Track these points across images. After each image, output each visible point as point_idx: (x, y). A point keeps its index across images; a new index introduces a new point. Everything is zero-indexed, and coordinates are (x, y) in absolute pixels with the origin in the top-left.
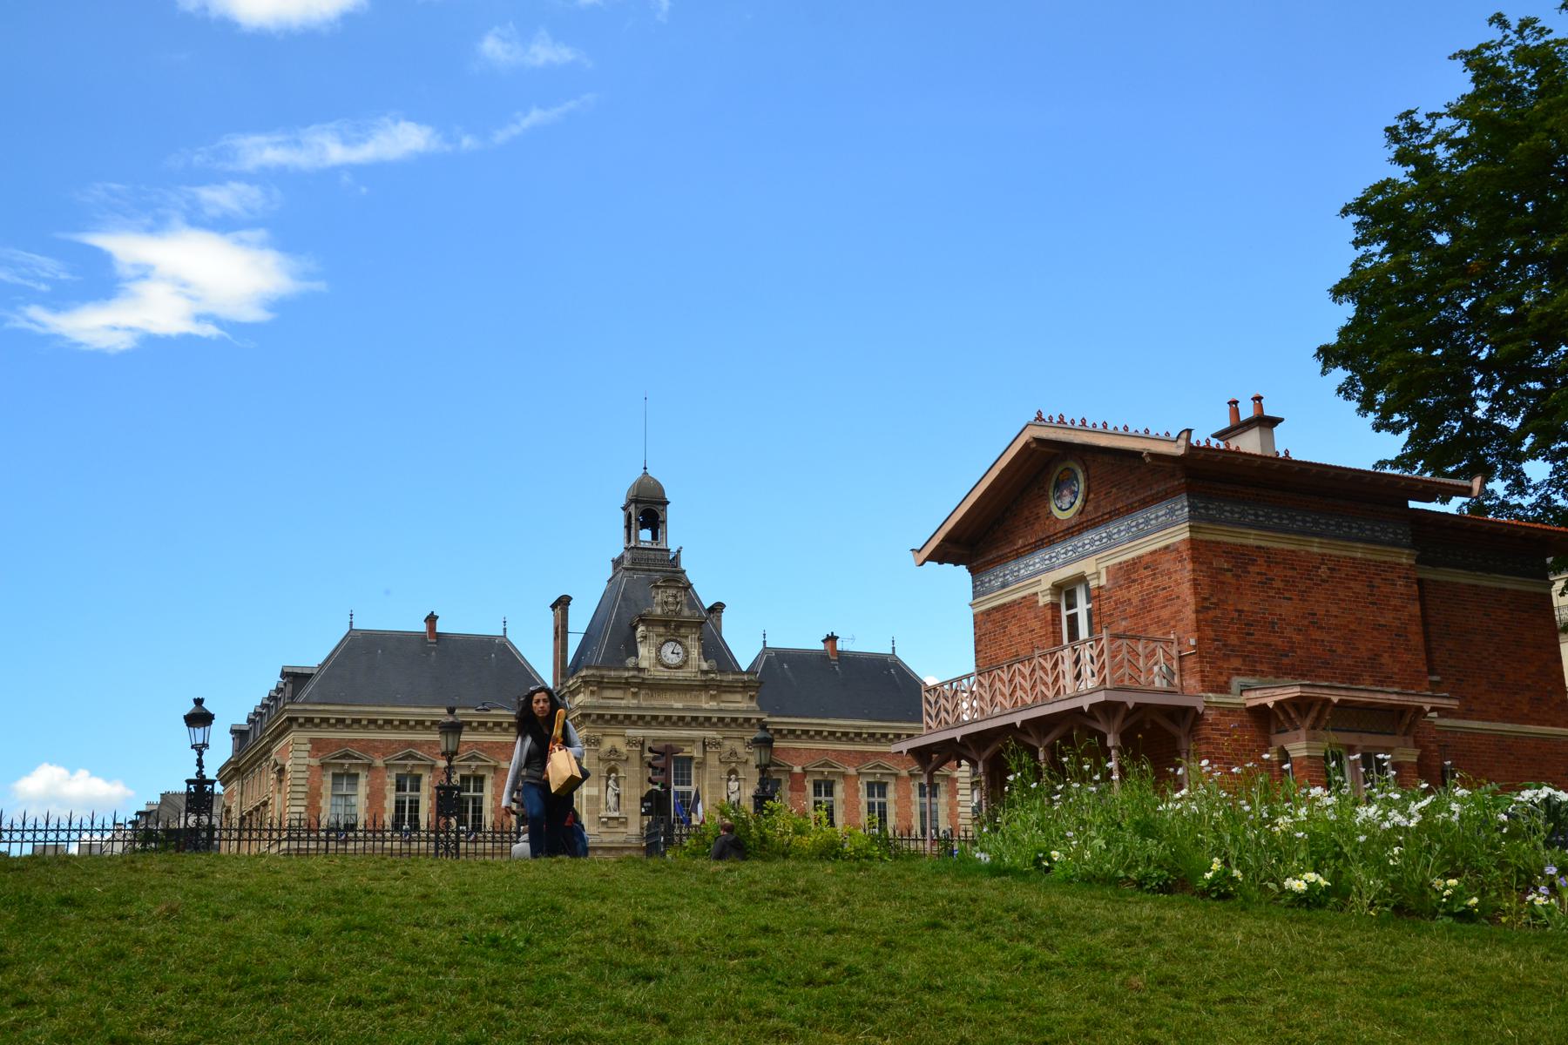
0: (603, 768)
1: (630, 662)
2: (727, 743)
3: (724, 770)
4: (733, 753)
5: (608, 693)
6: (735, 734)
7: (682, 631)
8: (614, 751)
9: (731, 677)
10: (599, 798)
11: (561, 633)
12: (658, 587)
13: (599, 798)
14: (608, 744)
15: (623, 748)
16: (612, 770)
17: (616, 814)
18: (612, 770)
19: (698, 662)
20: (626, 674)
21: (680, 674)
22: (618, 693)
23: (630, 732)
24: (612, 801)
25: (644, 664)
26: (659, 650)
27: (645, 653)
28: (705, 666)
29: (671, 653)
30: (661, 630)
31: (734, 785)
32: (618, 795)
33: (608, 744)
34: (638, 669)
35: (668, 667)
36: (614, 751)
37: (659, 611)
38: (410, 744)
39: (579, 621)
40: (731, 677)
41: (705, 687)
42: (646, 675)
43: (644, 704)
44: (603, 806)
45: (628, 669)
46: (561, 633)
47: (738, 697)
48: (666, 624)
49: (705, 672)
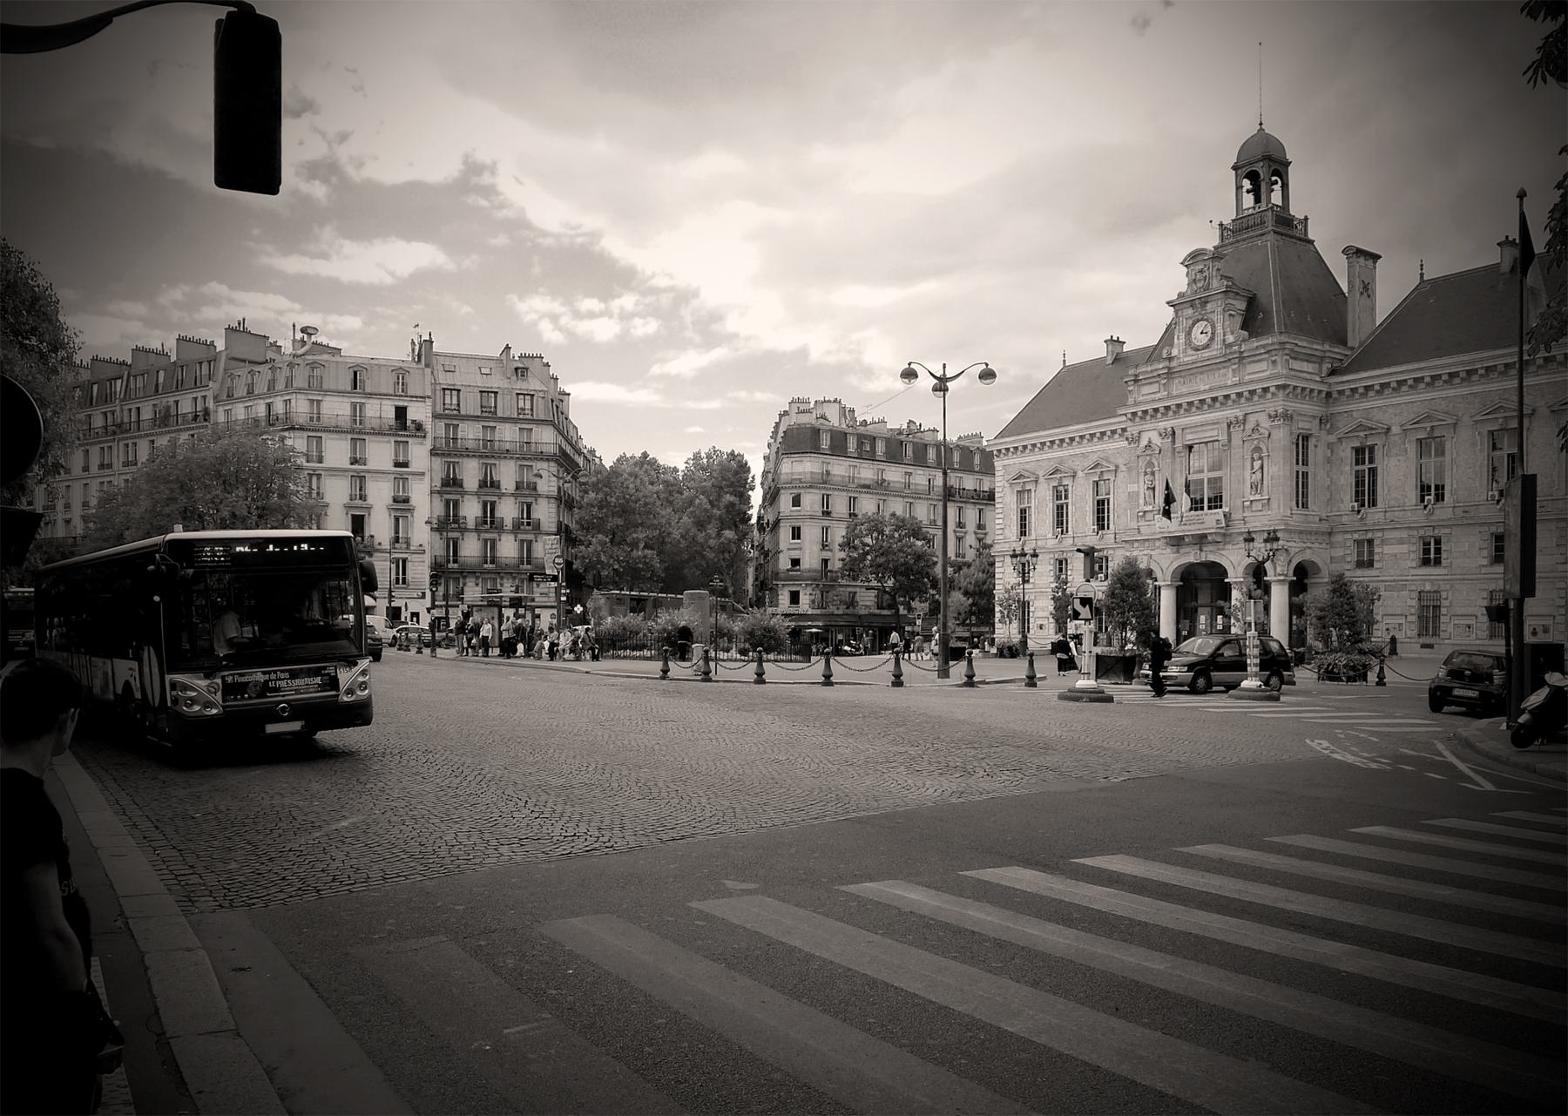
5: (1146, 390)
6: (1258, 408)
7: (1209, 306)
15: (1157, 440)
22: (1155, 388)
23: (1162, 425)
25: (1175, 352)
28: (1230, 339)
30: (1190, 311)
34: (1170, 359)
36: (1148, 446)
38: (1061, 460)
43: (1175, 393)
44: (1142, 501)
47: (1264, 365)
48: (1192, 304)
49: (1230, 345)
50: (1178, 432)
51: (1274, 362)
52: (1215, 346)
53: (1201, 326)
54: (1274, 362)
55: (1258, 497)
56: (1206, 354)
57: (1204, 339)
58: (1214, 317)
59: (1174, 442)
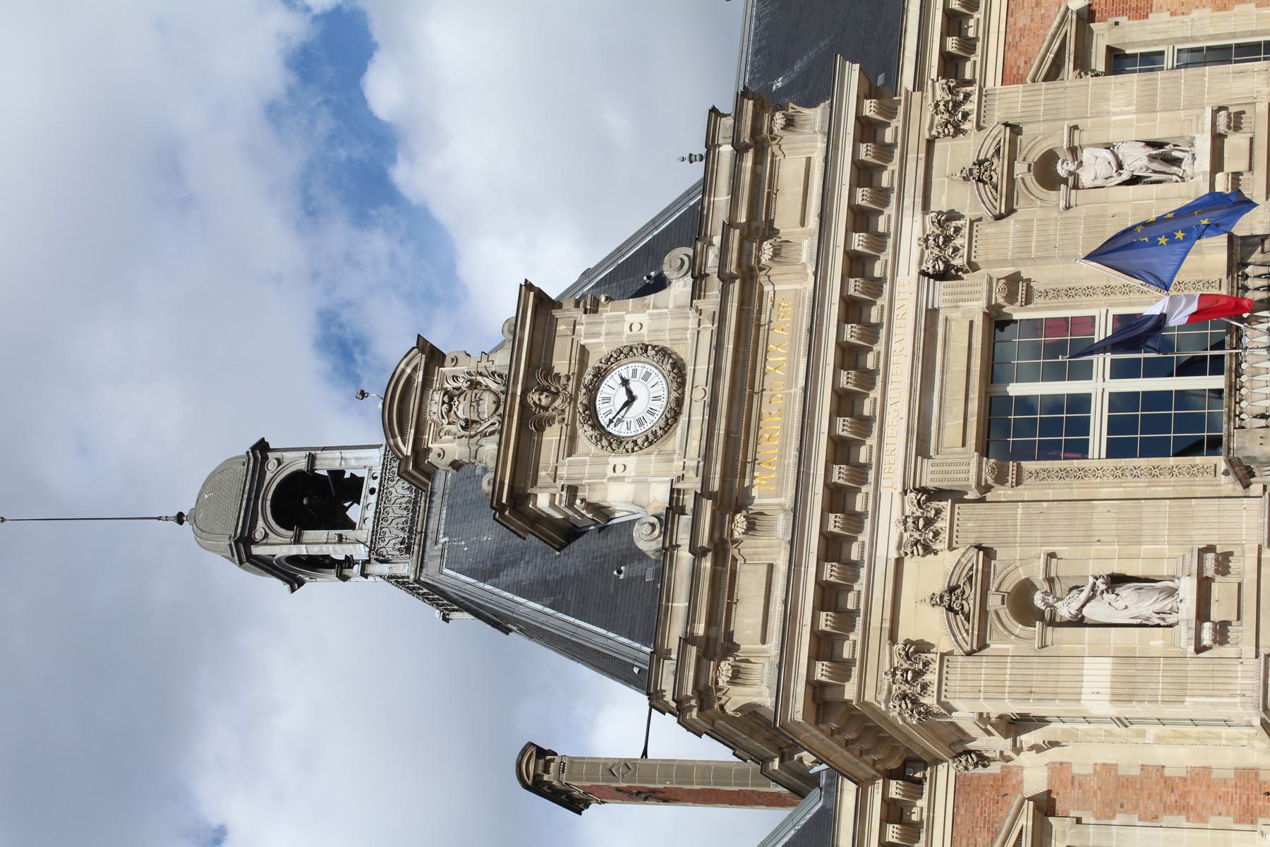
0: (1010, 640)
1: (647, 541)
2: (940, 202)
3: (1039, 207)
4: (979, 173)
7: (561, 364)
8: (950, 599)
9: (722, 198)
10: (1125, 658)
11: (644, 784)
12: (420, 452)
13: (1125, 658)
14: (925, 622)
16: (1023, 604)
17: (1188, 589)
18: (1023, 604)
19: (673, 316)
20: (684, 556)
21: (699, 372)
22: (749, 585)
24: (1129, 603)
25: (659, 497)
26: (615, 443)
27: (632, 487)
28: (680, 288)
29: (634, 398)
30: (552, 436)
31: (1095, 166)
32: (1116, 581)
33: (925, 622)
35: (675, 412)
36: (950, 599)
37: (489, 447)
39: (617, 723)
40: (722, 198)
41: (748, 277)
42: (692, 484)
44: (1156, 641)
45: (669, 549)
46: (644, 784)
48: (531, 424)
49: (699, 278)
50: (929, 480)
51: (790, 123)
52: (684, 351)
53: (610, 395)
54: (790, 123)
55: (1203, 145)
56: (699, 372)
57: (652, 390)
58: (600, 348)
59: (956, 496)
